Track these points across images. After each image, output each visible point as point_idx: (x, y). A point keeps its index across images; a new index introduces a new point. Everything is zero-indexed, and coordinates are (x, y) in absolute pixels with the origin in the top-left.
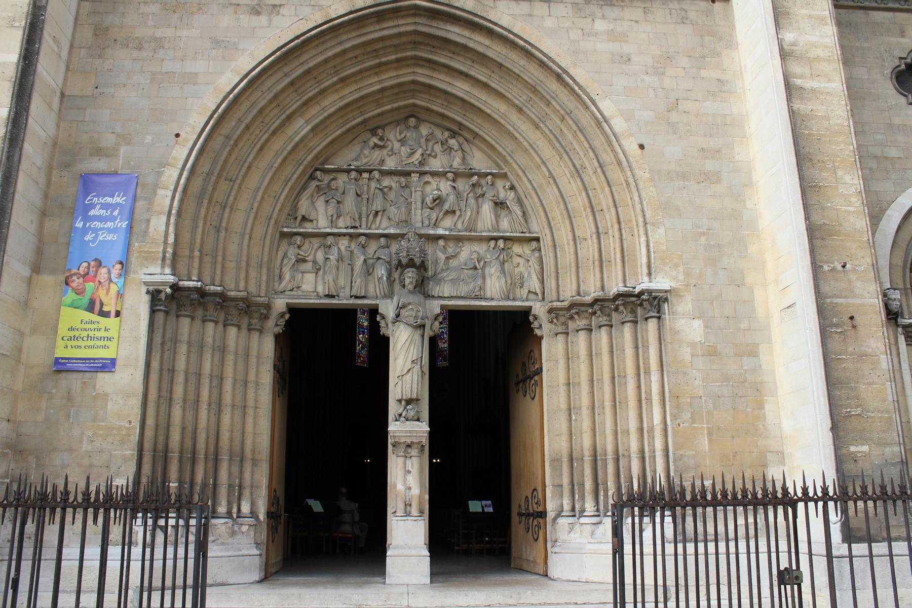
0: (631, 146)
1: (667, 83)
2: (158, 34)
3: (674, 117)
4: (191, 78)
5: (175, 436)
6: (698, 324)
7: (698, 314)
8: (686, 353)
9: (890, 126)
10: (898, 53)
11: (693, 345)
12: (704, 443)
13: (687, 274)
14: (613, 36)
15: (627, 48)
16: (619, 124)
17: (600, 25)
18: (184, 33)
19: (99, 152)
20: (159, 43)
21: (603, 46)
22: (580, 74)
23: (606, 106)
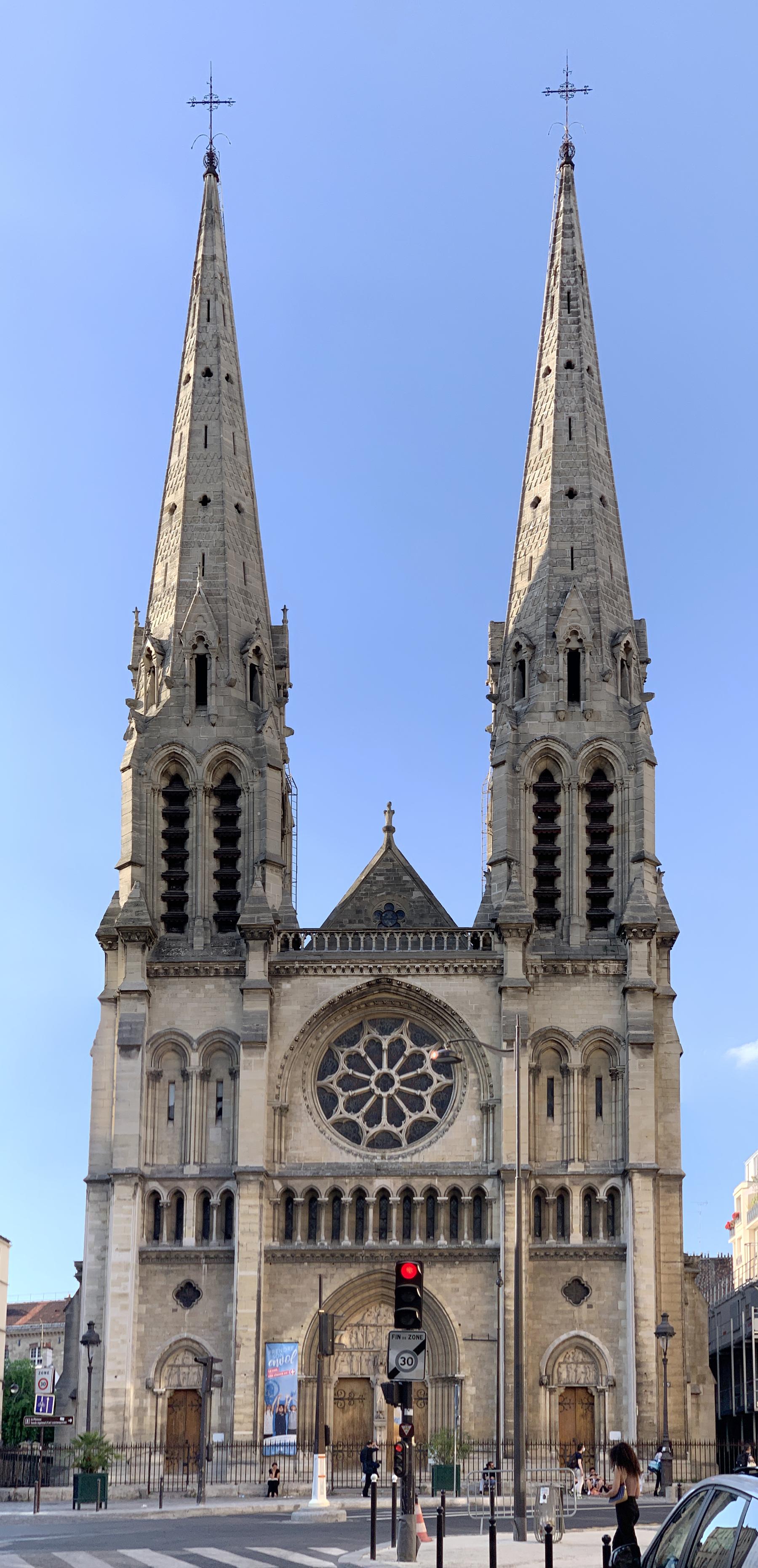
0: (456, 1324)
1: (472, 1299)
2: (293, 1287)
3: (473, 1312)
4: (304, 1304)
5: (307, 1426)
6: (474, 1388)
7: (474, 1384)
8: (469, 1398)
9: (557, 1311)
10: (566, 1280)
11: (471, 1396)
12: (473, 1428)
13: (472, 1371)
14: (453, 1281)
15: (457, 1285)
16: (452, 1317)
17: (449, 1276)
18: (301, 1286)
19: (277, 1333)
20: (292, 1290)
21: (448, 1286)
22: (440, 1297)
23: (448, 1310)
